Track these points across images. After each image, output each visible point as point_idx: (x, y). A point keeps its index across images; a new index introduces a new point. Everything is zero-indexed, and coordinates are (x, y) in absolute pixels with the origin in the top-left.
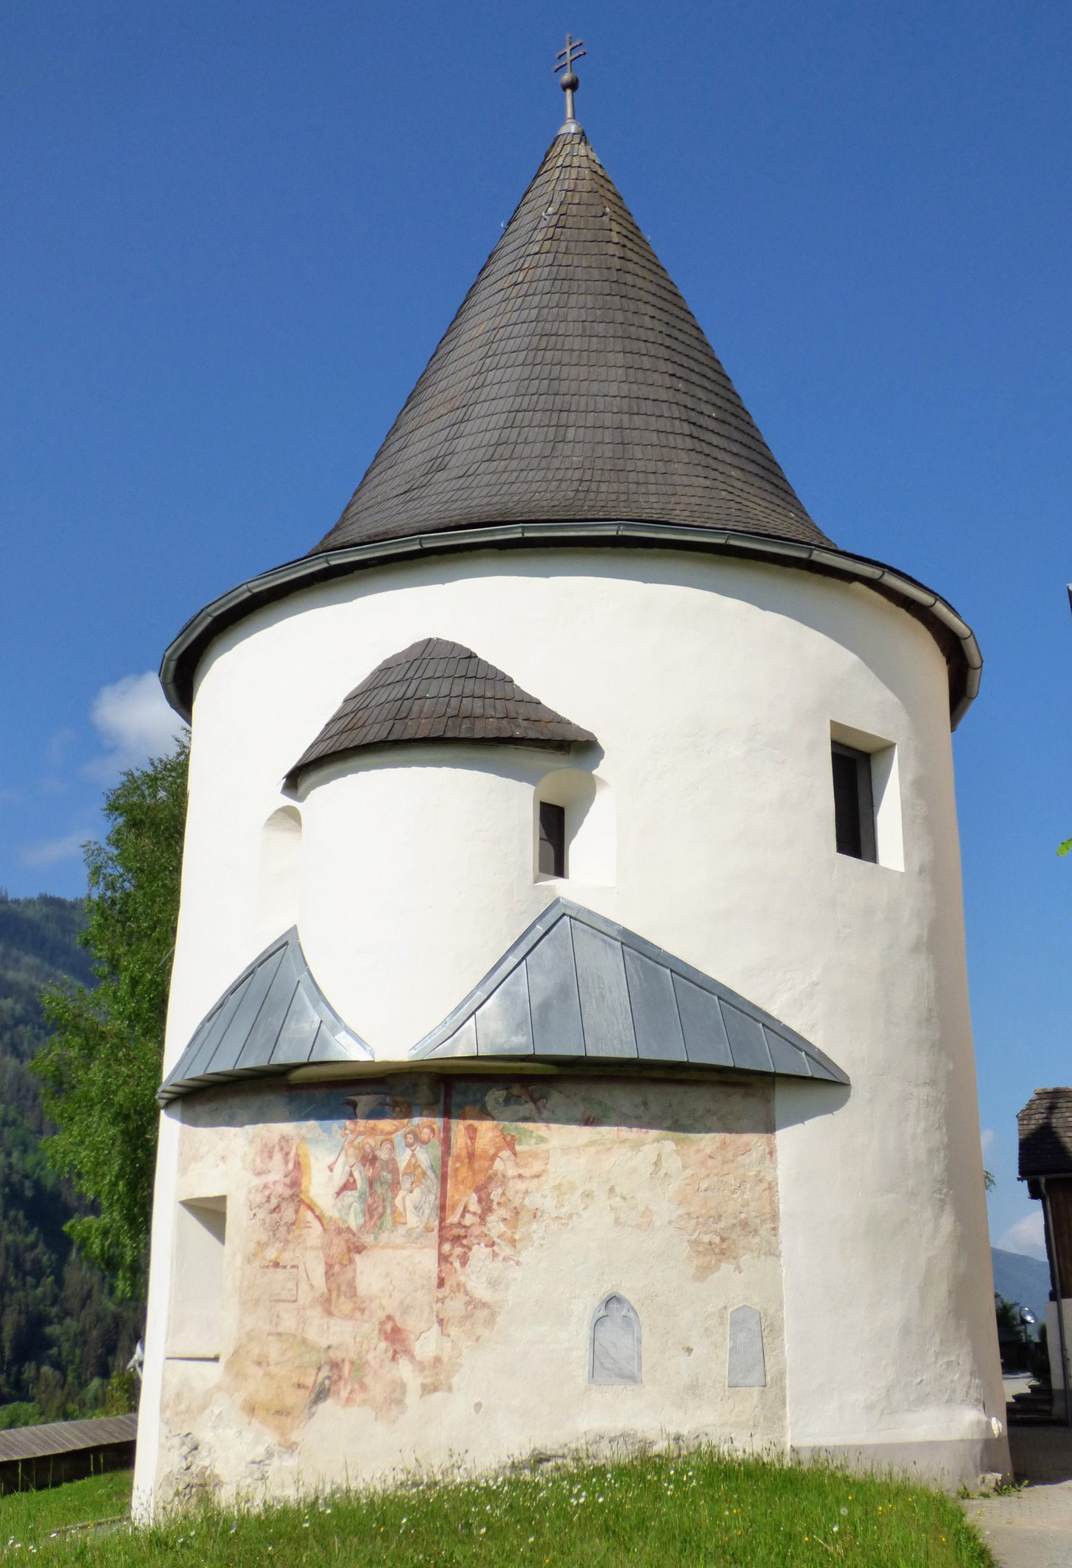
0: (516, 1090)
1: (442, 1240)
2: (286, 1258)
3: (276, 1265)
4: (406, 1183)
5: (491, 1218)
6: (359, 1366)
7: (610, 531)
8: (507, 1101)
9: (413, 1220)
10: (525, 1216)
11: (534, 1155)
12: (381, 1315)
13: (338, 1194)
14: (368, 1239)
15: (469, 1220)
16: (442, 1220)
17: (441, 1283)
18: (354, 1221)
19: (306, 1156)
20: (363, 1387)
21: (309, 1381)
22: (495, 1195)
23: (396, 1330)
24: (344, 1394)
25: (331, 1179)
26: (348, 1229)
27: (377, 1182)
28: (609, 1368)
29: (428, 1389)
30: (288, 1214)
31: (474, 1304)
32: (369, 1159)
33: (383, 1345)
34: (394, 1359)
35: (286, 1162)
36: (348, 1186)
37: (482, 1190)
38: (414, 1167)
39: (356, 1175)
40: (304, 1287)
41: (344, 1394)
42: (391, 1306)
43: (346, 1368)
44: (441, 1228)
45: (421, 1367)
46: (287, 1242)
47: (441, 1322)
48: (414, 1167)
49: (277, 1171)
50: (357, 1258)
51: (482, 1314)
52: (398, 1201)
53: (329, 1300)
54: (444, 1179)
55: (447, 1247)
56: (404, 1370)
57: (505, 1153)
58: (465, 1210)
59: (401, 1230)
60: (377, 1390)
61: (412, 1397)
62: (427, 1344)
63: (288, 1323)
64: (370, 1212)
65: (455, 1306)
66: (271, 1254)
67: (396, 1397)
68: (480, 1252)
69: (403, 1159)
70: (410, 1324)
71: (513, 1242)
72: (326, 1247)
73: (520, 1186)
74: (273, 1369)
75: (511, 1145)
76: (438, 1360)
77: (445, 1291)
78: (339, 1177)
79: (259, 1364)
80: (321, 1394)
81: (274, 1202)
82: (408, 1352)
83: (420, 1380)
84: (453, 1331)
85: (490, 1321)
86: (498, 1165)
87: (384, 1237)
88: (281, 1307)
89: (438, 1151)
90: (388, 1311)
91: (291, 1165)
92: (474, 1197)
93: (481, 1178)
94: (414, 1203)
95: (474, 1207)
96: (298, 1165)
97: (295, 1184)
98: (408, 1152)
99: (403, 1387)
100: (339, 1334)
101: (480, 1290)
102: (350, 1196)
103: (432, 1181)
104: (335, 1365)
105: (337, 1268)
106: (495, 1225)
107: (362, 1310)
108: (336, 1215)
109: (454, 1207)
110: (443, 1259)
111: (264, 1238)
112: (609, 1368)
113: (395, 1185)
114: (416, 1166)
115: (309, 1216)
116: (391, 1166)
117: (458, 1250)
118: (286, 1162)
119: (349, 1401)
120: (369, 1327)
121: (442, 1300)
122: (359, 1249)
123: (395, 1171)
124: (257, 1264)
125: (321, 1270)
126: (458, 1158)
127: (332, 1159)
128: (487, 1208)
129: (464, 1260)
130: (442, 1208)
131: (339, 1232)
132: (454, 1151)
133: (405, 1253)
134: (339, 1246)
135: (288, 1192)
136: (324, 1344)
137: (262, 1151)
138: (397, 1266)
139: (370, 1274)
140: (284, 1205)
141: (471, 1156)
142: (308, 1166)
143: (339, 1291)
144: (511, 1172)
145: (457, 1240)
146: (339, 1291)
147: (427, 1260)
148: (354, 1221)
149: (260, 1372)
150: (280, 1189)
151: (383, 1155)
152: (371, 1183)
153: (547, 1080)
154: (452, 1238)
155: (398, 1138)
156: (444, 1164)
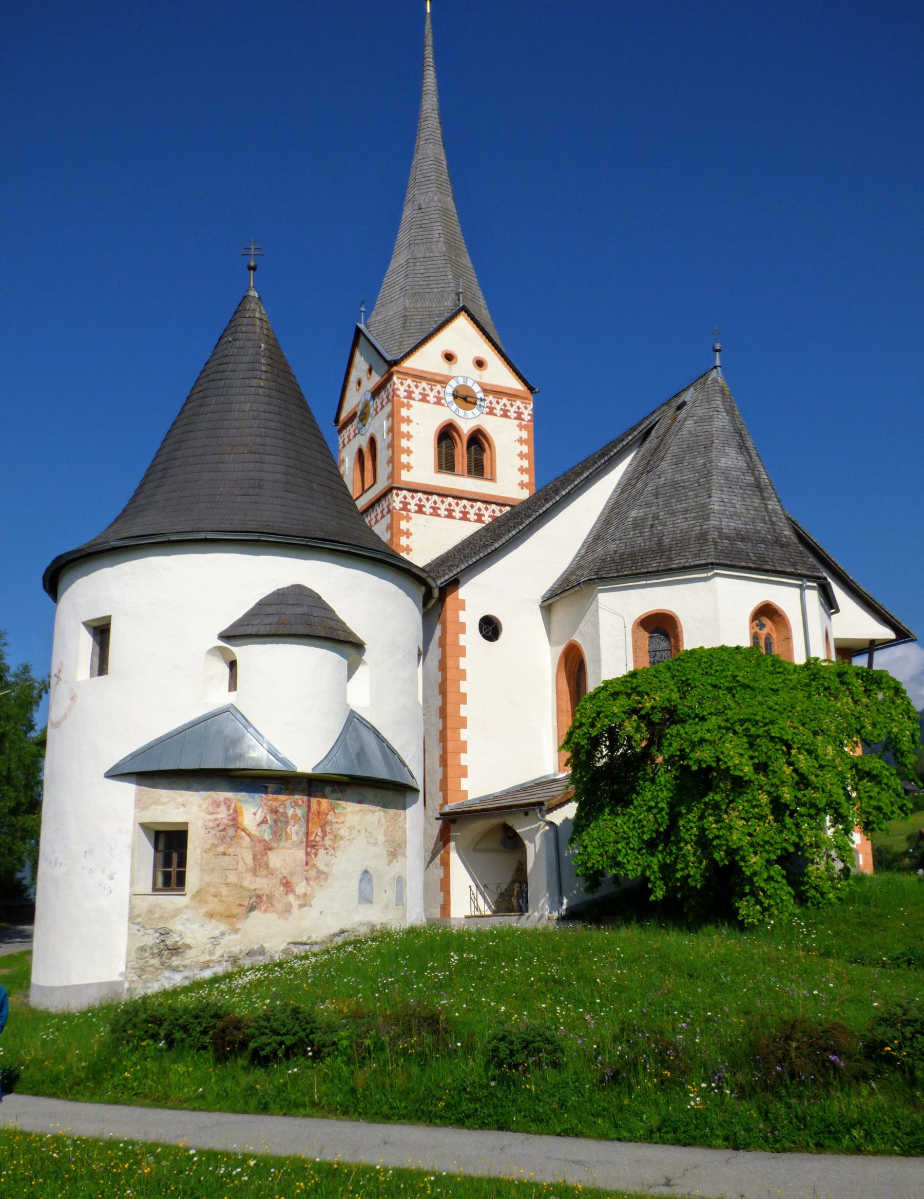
0: (336, 787)
1: (307, 846)
2: (231, 851)
3: (224, 854)
4: (292, 823)
5: (326, 838)
6: (270, 897)
7: (378, 556)
8: (332, 792)
9: (294, 838)
10: (338, 838)
11: (341, 814)
12: (281, 876)
13: (258, 825)
14: (275, 845)
15: (318, 839)
16: (307, 838)
17: (307, 864)
18: (267, 837)
19: (241, 808)
20: (272, 905)
21: (246, 903)
22: (328, 829)
23: (288, 883)
24: (263, 908)
25: (254, 819)
26: (265, 840)
27: (278, 822)
28: (365, 899)
29: (301, 906)
30: (231, 832)
31: (321, 872)
32: (274, 811)
33: (282, 888)
34: (286, 894)
35: (229, 810)
36: (264, 822)
37: (323, 827)
38: (295, 816)
39: (268, 817)
40: (241, 864)
41: (263, 908)
42: (285, 873)
43: (264, 898)
44: (307, 842)
45: (298, 897)
46: (231, 844)
47: (307, 879)
48: (295, 816)
49: (223, 814)
50: (269, 852)
51: (322, 876)
52: (288, 830)
53: (255, 870)
54: (308, 821)
55: (309, 849)
56: (291, 898)
57: (331, 813)
58: (316, 835)
59: (290, 842)
60: (279, 906)
61: (295, 910)
62: (301, 888)
63: (233, 878)
64: (275, 833)
65: (313, 873)
66: (221, 849)
67: (287, 910)
68: (322, 852)
69: (290, 812)
70: (294, 880)
71: (334, 849)
72: (253, 848)
73: (337, 826)
74: (224, 898)
75: (333, 809)
76: (305, 894)
77: (308, 867)
78: (259, 817)
79: (216, 896)
80: (252, 908)
81: (222, 827)
82: (293, 891)
83: (298, 902)
84: (311, 883)
85: (326, 880)
86: (329, 817)
87: (282, 844)
88: (227, 872)
89: (306, 809)
90: (285, 874)
91: (231, 811)
92: (320, 830)
93: (322, 822)
94: (295, 831)
95: (320, 834)
96: (236, 811)
97: (234, 819)
98: (292, 810)
99: (291, 905)
100: (261, 884)
101: (322, 867)
102: (264, 827)
103: (303, 822)
104: (259, 897)
105: (259, 856)
106: (328, 842)
107: (272, 874)
108: (257, 834)
109: (312, 834)
110: (308, 854)
111: (216, 842)
112: (365, 899)
113: (287, 823)
114: (296, 816)
115: (243, 834)
116: (285, 815)
117: (314, 851)
118: (229, 810)
119: (266, 911)
120: (275, 881)
121: (307, 871)
122: (270, 849)
123: (286, 817)
124: (211, 854)
125: (251, 857)
126: (314, 813)
127: (254, 810)
128: (325, 834)
129: (316, 855)
130: (307, 834)
131: (260, 841)
132: (312, 810)
133: (292, 851)
134: (259, 847)
135: (231, 823)
136: (253, 887)
137: (212, 804)
138: (287, 857)
139: (276, 859)
140: (228, 828)
141: (319, 813)
142: (242, 812)
143: (259, 865)
144: (334, 820)
145: (313, 847)
146: (259, 865)
147: (301, 854)
148: (267, 837)
149: (216, 900)
150: (226, 821)
151: (281, 810)
152: (275, 822)
153: (346, 784)
154: (311, 846)
155: (288, 803)
156: (308, 816)
